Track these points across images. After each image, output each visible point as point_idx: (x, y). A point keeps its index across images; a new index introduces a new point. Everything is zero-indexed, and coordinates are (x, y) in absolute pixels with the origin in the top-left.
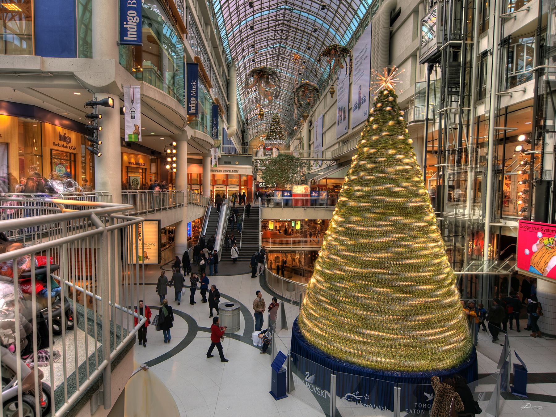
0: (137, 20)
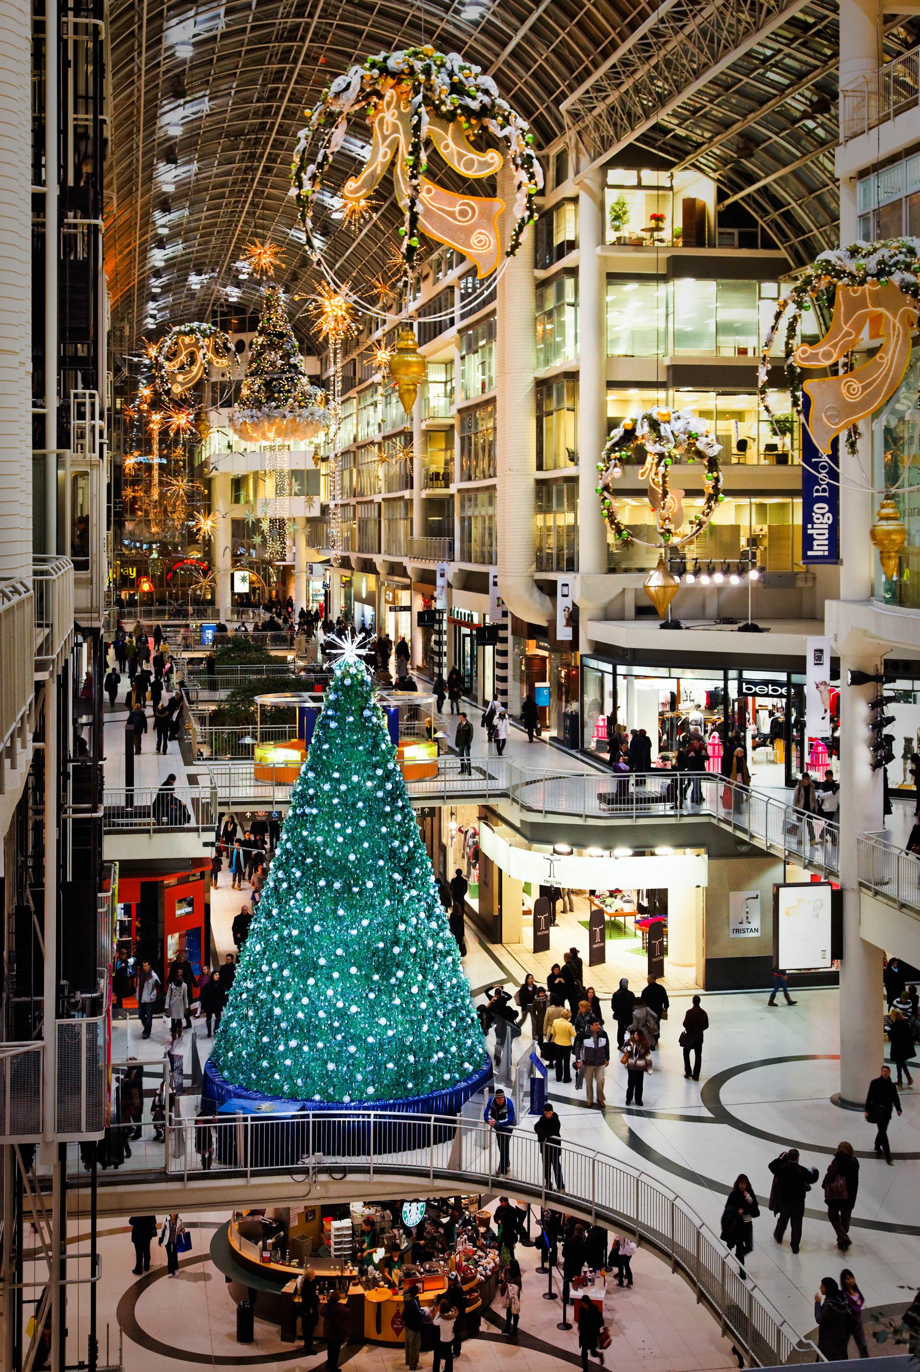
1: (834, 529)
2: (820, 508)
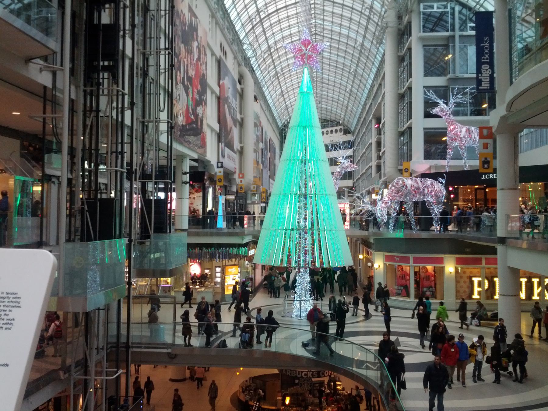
0: (489, 72)
2: (485, 67)
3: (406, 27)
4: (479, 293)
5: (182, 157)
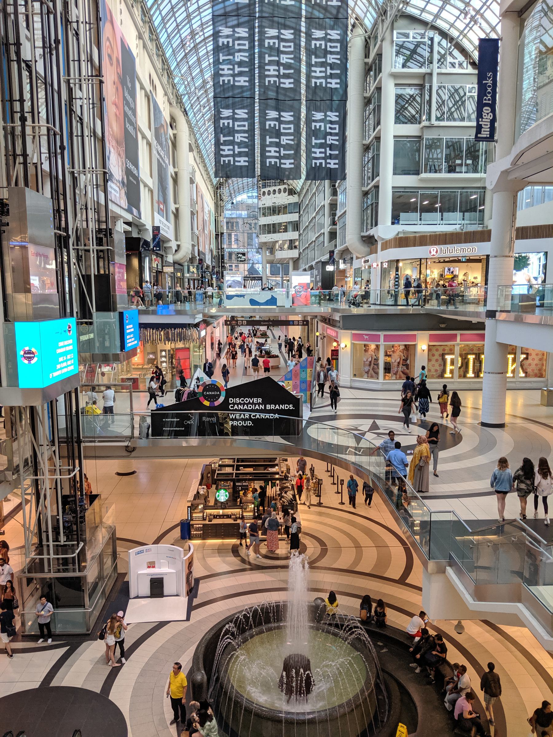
1: (493, 121)
3: (374, 60)
4: (452, 372)
5: (116, 218)
